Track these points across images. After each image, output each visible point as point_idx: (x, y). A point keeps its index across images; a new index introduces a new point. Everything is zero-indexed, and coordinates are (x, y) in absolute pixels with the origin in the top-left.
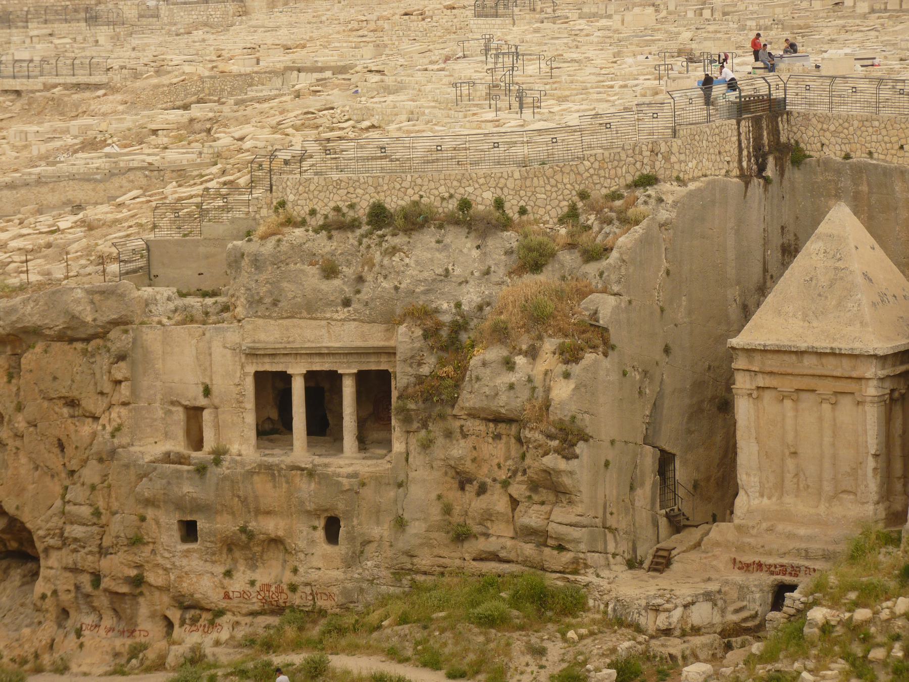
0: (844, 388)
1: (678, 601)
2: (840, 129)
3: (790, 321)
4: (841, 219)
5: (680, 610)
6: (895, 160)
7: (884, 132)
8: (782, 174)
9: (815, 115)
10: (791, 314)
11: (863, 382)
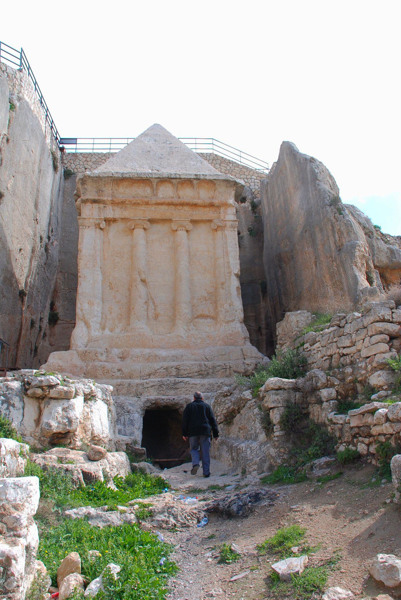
0: (201, 215)
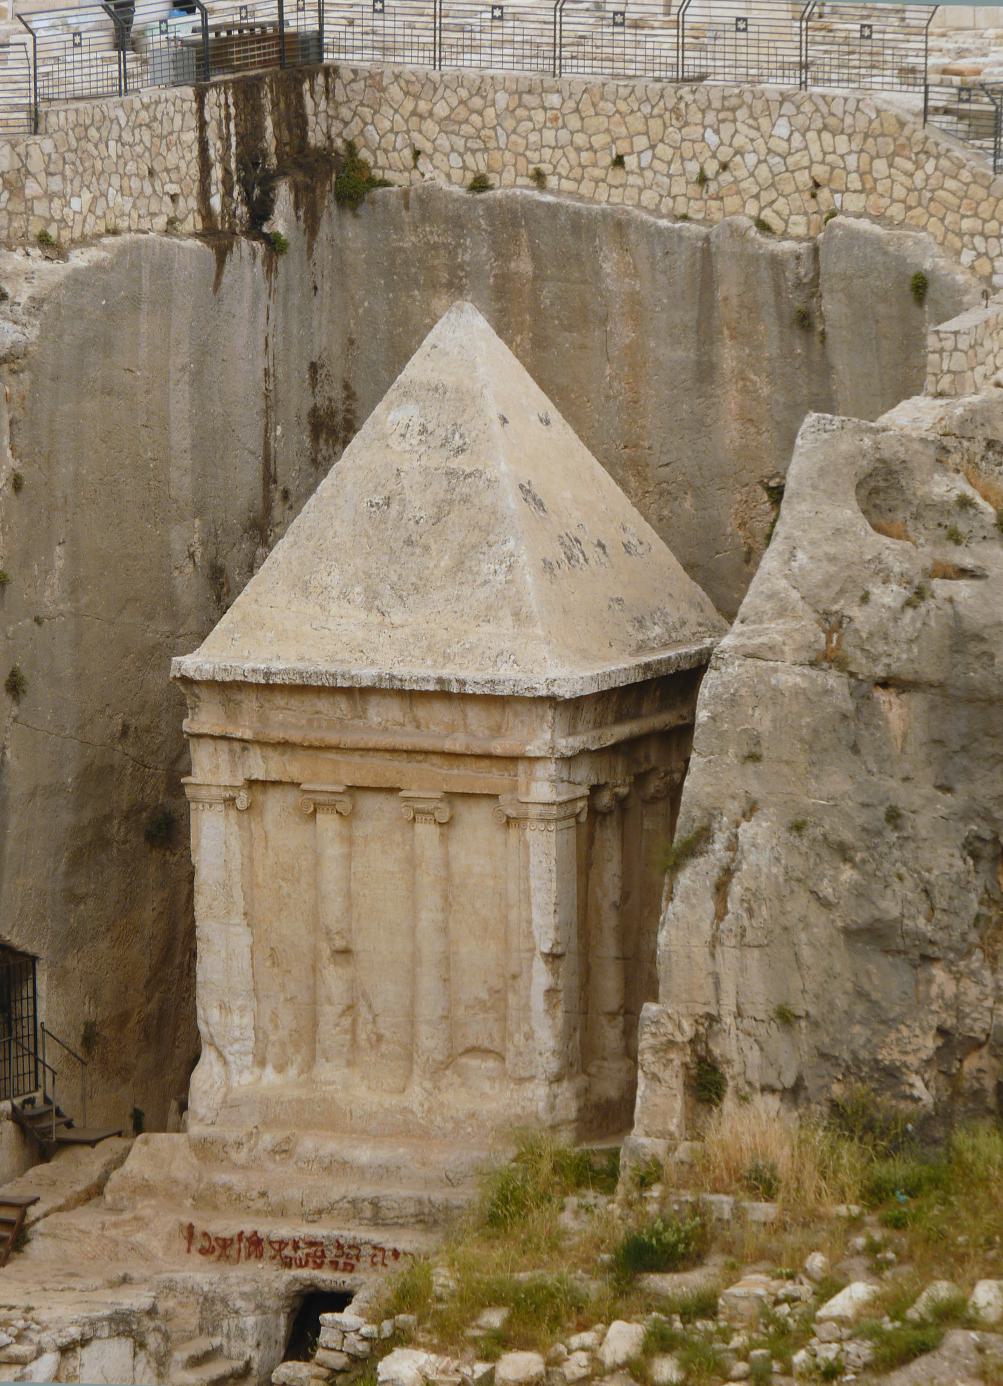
0: (472, 782)
1: (46, 1338)
2: (462, 112)
3: (334, 609)
4: (464, 346)
5: (50, 1360)
6: (602, 193)
7: (574, 122)
8: (312, 229)
9: (397, 77)
10: (334, 593)
11: (521, 767)
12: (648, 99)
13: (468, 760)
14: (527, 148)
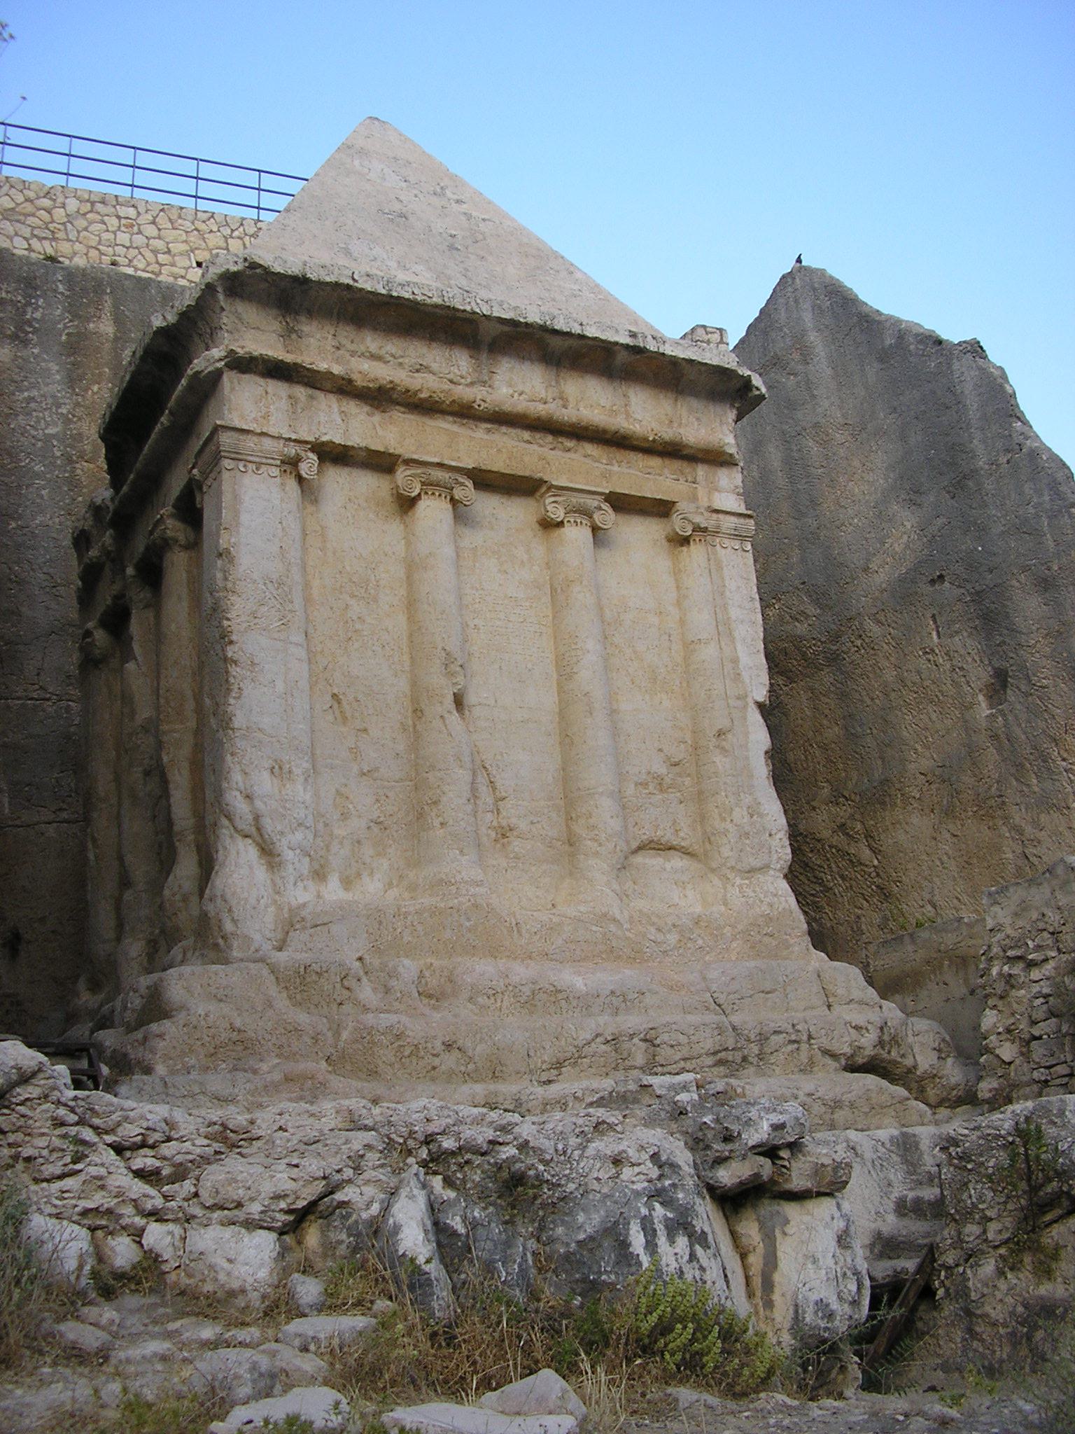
2: (29, 208)
7: (151, 231)
11: (701, 471)
12: (227, 224)
13: (632, 456)
14: (99, 243)
